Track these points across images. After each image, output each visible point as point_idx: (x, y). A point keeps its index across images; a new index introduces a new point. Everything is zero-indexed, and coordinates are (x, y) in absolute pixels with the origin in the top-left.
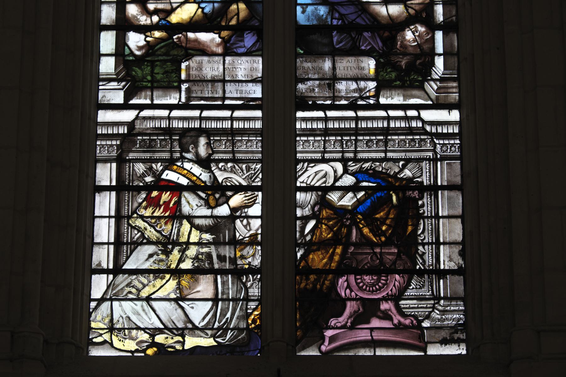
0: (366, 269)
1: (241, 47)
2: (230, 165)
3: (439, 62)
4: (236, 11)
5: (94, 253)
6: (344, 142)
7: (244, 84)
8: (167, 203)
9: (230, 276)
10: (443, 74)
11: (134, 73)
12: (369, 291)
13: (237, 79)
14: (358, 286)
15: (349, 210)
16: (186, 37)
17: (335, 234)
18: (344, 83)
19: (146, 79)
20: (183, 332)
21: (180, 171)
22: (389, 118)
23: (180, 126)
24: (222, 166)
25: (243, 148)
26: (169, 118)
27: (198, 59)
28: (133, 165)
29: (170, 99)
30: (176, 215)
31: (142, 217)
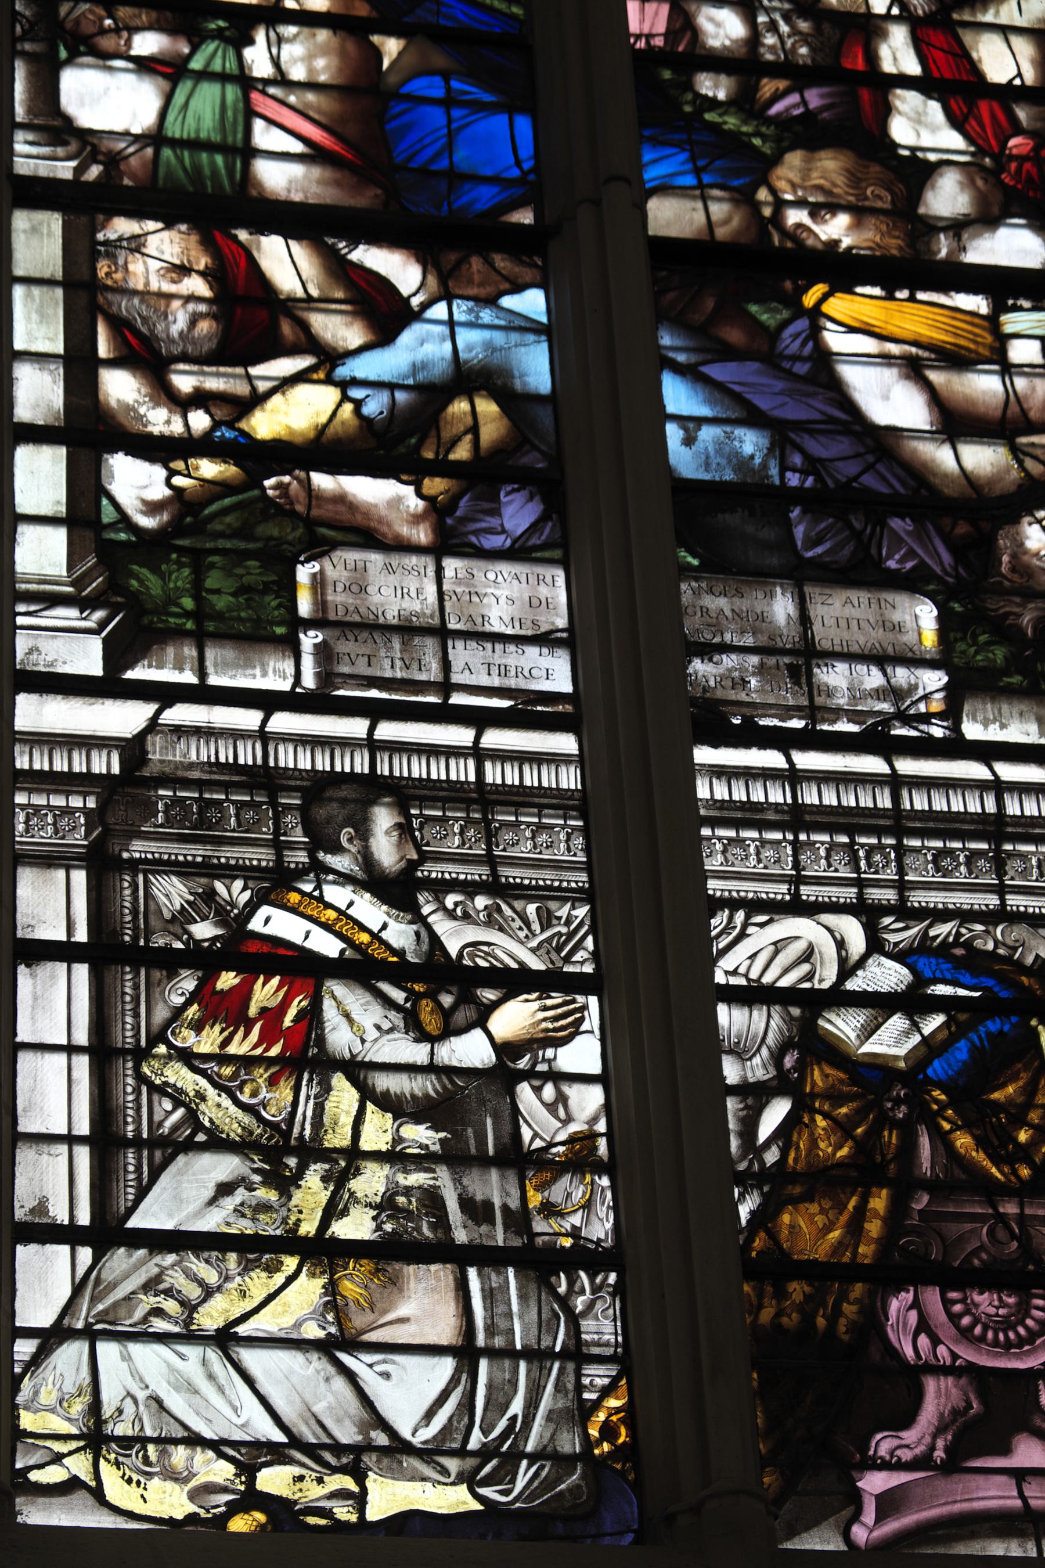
0: (975, 1269)
1: (491, 531)
2: (481, 902)
4: (469, 420)
5: (18, 1170)
6: (861, 853)
7: (511, 648)
8: (272, 1016)
9: (511, 1272)
11: (134, 583)
12: (996, 1343)
13: (488, 628)
14: (957, 1326)
15: (898, 1072)
16: (307, 484)
17: (860, 1146)
18: (842, 667)
20: (358, 1460)
21: (314, 908)
22: (999, 787)
23: (304, 762)
24: (456, 904)
25: (524, 850)
26: (263, 736)
27: (352, 556)
28: (146, 881)
29: (264, 674)
30: (307, 1057)
31: (187, 1057)
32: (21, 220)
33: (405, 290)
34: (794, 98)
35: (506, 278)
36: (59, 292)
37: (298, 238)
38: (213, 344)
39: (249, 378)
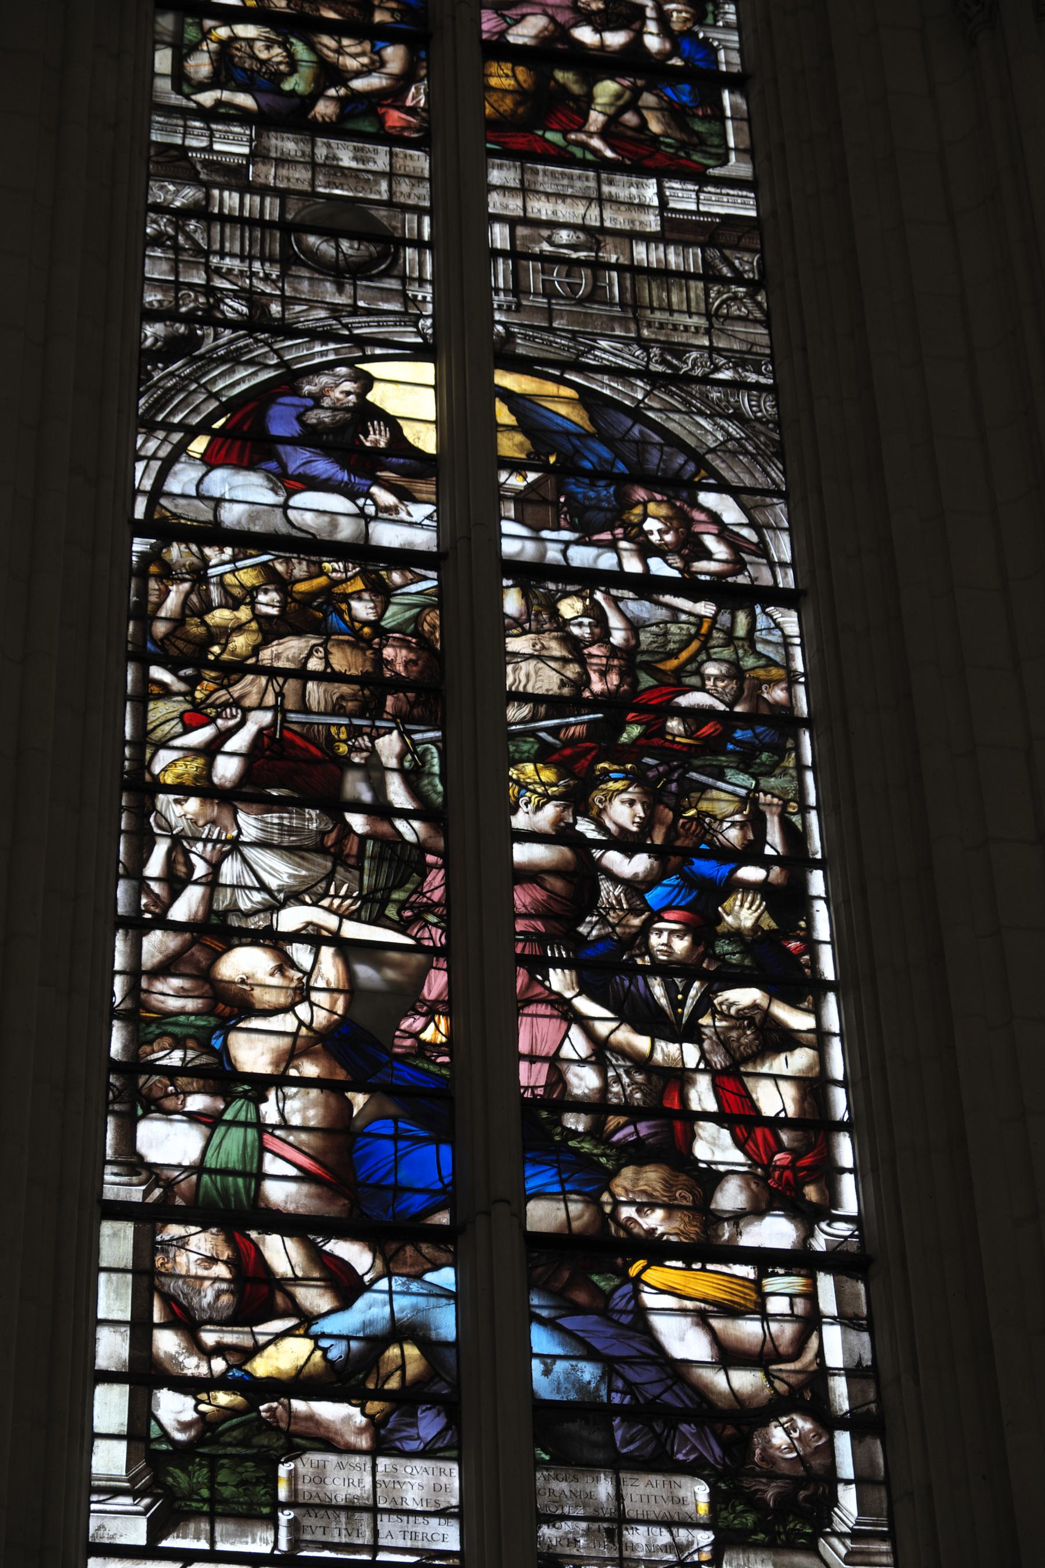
1: (410, 1438)
3: (848, 1498)
4: (399, 1361)
7: (420, 1519)
10: (857, 1524)
11: (170, 1479)
13: (405, 1506)
16: (288, 1408)
18: (642, 1529)
19: (198, 1494)
27: (316, 1457)
29: (254, 1541)
32: (107, 1228)
33: (360, 1272)
34: (630, 1129)
35: (429, 1260)
36: (129, 1277)
37: (290, 1236)
38: (230, 1312)
39: (253, 1334)
